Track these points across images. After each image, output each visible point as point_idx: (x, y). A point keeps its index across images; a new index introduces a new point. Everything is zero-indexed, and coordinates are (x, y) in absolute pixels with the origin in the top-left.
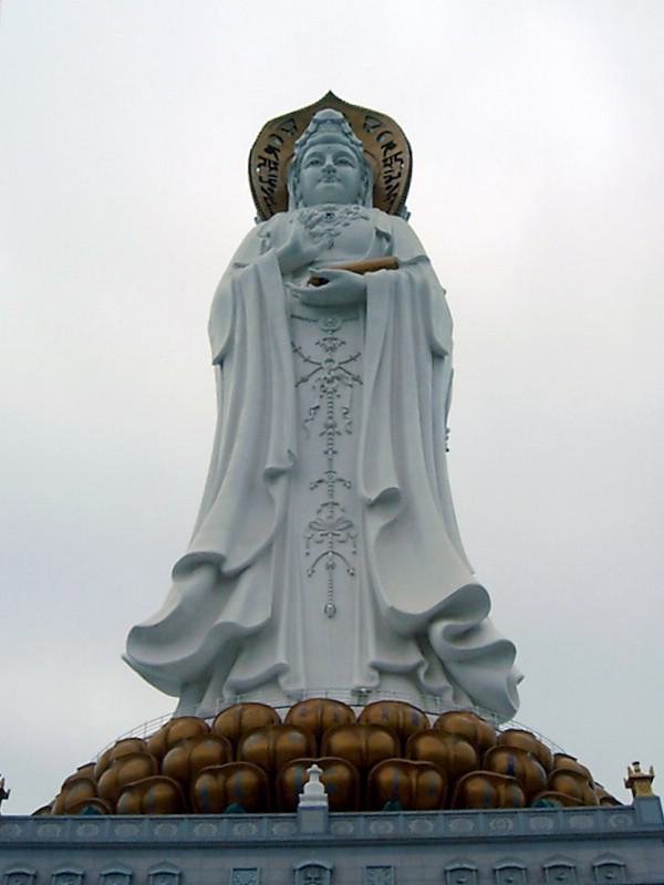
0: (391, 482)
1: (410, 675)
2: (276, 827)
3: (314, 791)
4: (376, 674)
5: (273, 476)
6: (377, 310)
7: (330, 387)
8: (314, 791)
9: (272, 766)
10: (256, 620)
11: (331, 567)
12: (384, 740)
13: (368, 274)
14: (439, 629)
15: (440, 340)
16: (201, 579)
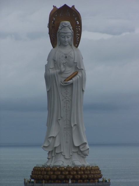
0: (76, 124)
1: (77, 152)
2: (67, 184)
3: (70, 181)
4: (73, 153)
5: (59, 119)
6: (74, 86)
7: (66, 101)
8: (70, 181)
9: (65, 175)
10: (58, 145)
11: (67, 135)
12: (75, 173)
13: (74, 79)
14: (81, 147)
15: (84, 90)
16: (52, 138)
